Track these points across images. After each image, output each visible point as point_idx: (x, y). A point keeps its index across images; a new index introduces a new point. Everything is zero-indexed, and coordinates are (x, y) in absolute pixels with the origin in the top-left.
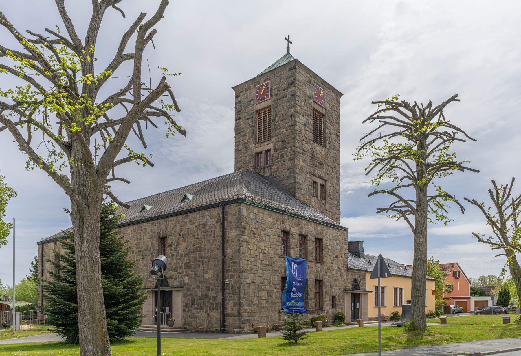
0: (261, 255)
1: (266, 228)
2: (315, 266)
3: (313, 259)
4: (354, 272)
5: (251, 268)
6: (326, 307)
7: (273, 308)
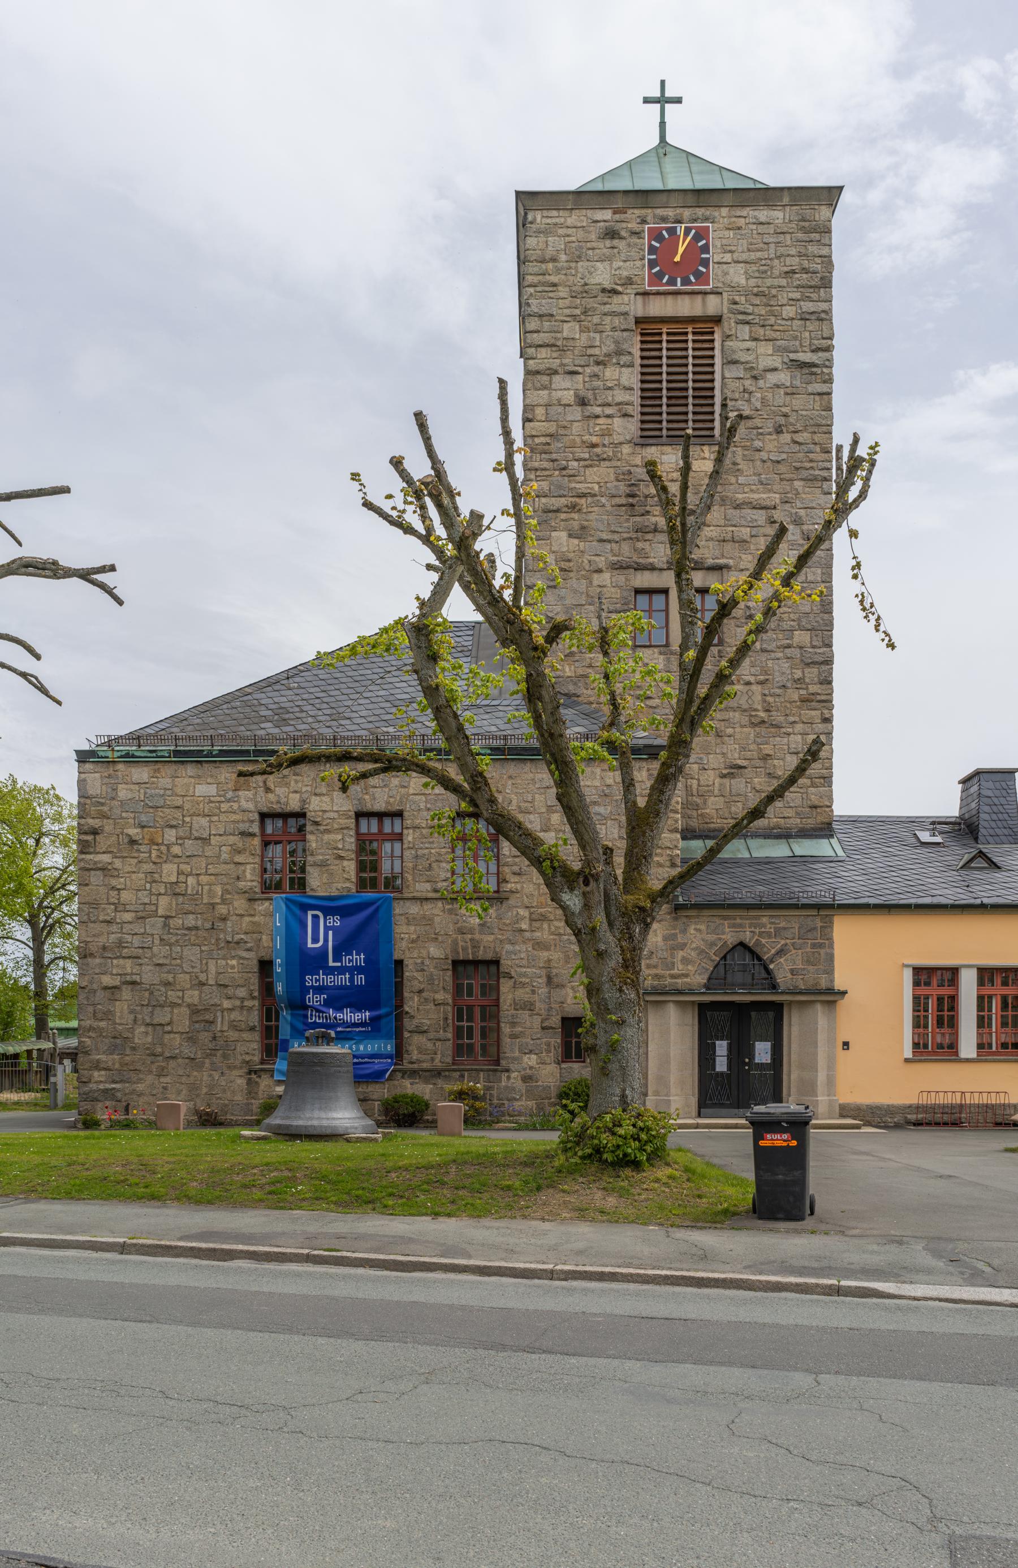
0: (163, 901)
1: (187, 819)
3: (436, 891)
4: (725, 918)
7: (218, 1059)
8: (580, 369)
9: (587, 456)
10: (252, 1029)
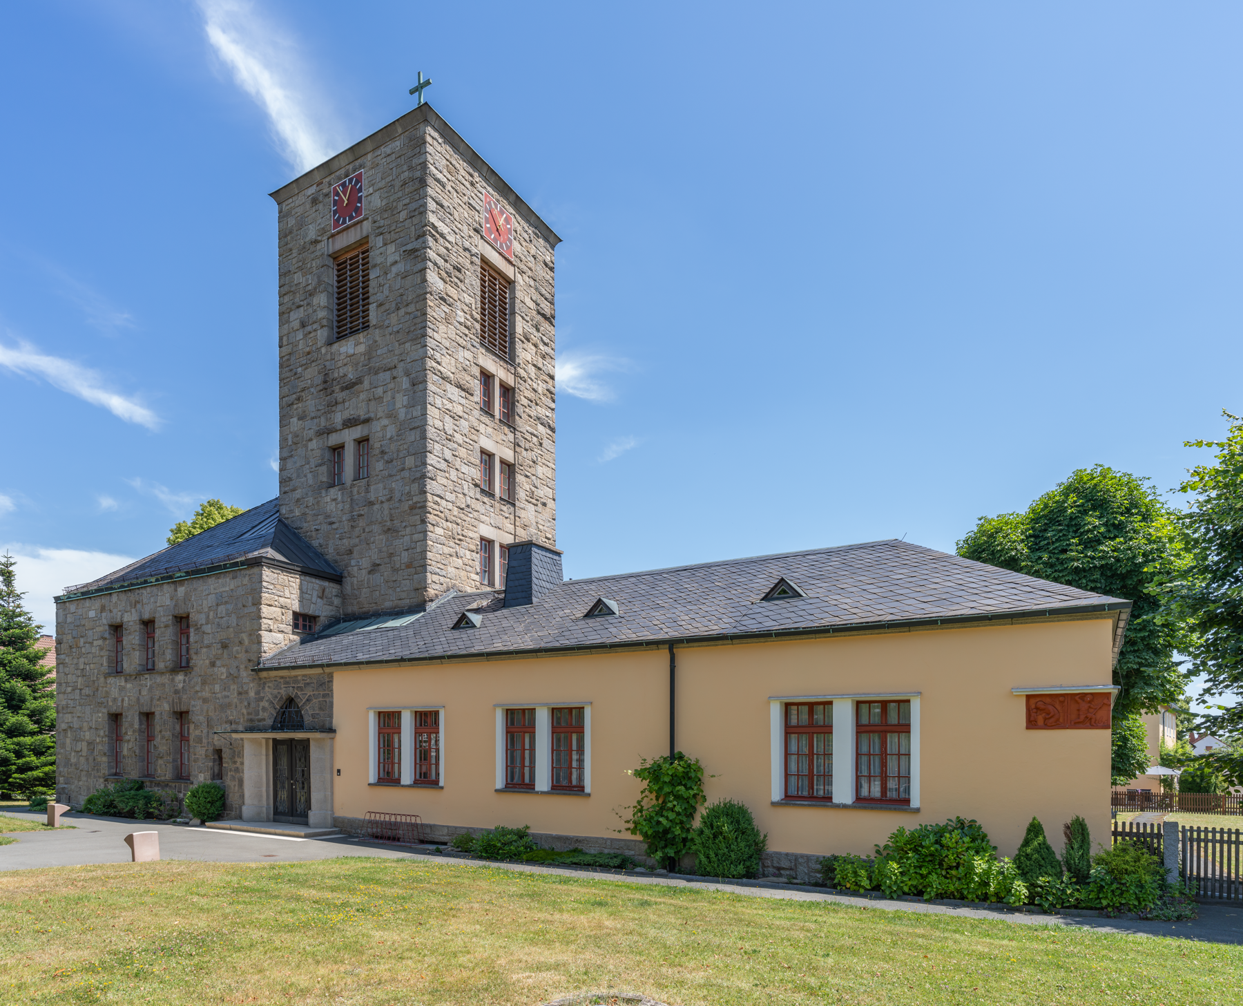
2: (173, 680)
5: (67, 704)
6: (196, 776)
8: (302, 303)
9: (304, 362)
10: (105, 754)
